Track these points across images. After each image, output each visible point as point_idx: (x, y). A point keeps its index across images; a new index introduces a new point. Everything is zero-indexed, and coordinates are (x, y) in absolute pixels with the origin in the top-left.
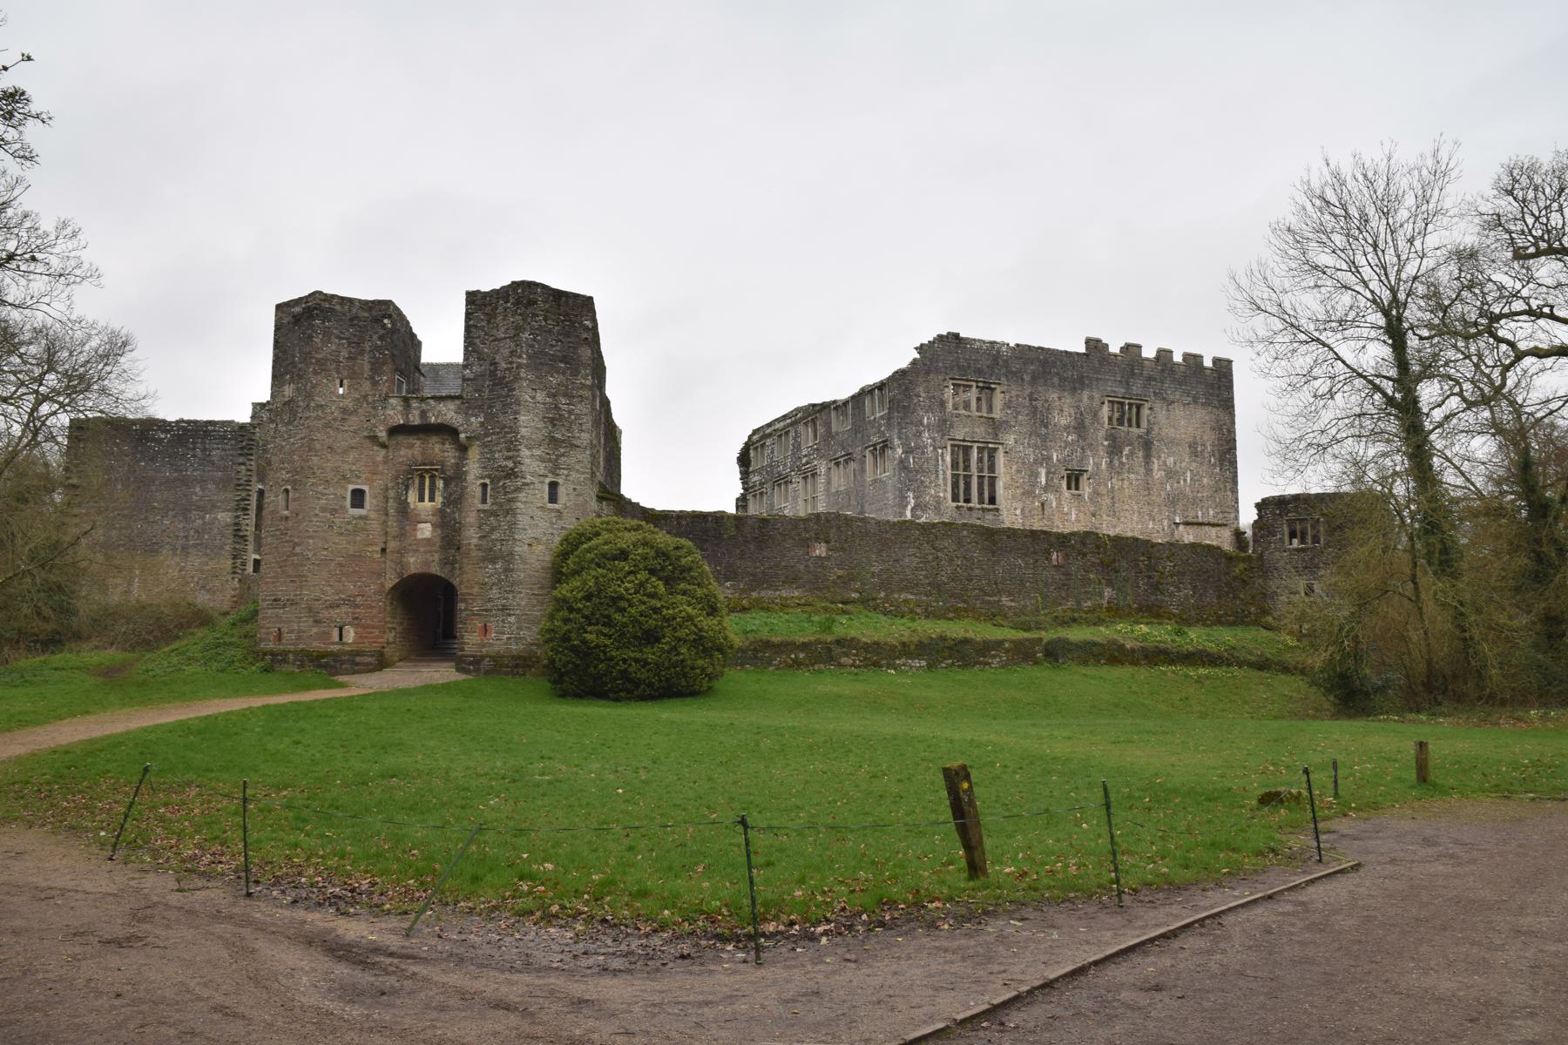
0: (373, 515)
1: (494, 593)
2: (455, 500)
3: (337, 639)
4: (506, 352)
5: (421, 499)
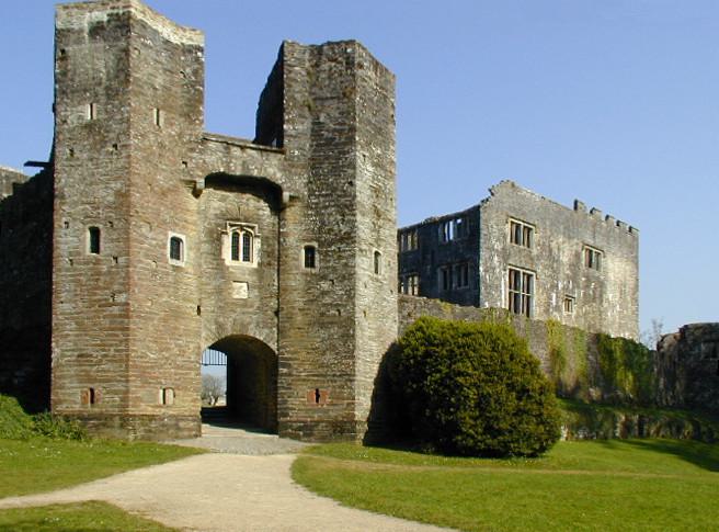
3: (162, 402)
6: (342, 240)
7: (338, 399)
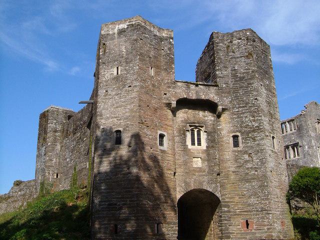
1: (253, 200)
3: (156, 232)
4: (243, 64)
6: (254, 131)
7: (260, 225)
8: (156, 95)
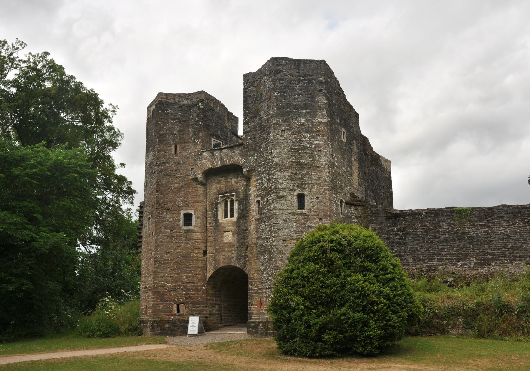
0: (198, 230)
2: (244, 214)
3: (175, 312)
5: (226, 216)
8: (181, 174)
